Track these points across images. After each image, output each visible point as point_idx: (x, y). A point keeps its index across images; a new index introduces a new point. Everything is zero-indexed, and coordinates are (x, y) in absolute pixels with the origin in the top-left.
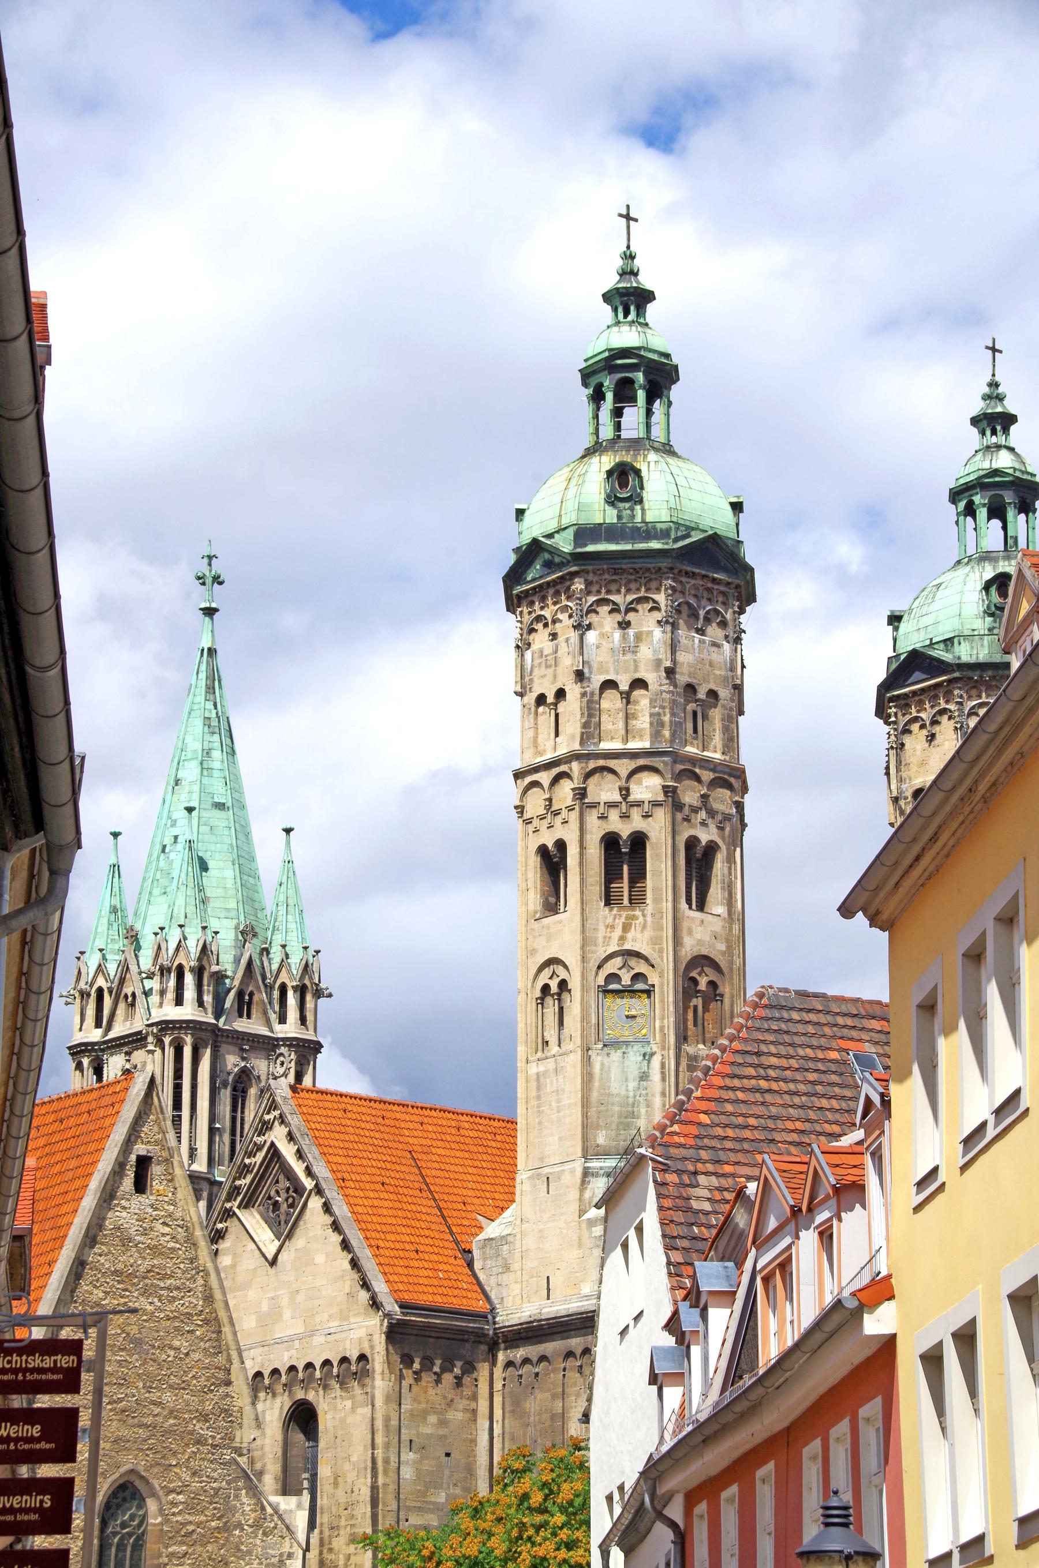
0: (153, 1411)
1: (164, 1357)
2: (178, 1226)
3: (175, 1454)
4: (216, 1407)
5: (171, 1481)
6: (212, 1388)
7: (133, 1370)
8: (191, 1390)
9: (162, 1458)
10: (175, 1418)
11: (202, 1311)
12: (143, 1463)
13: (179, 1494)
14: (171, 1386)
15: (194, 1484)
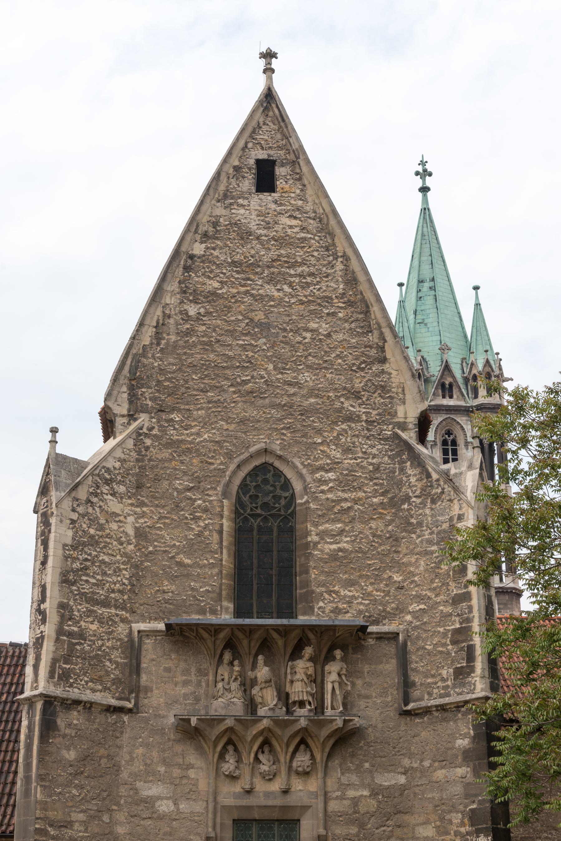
0: (287, 391)
1: (299, 339)
2: (309, 218)
3: (319, 432)
4: (369, 384)
5: (316, 459)
6: (363, 366)
7: (260, 353)
8: (336, 369)
9: (302, 437)
10: (317, 396)
11: (344, 294)
12: (278, 442)
13: (327, 471)
14: (309, 367)
15: (346, 461)
